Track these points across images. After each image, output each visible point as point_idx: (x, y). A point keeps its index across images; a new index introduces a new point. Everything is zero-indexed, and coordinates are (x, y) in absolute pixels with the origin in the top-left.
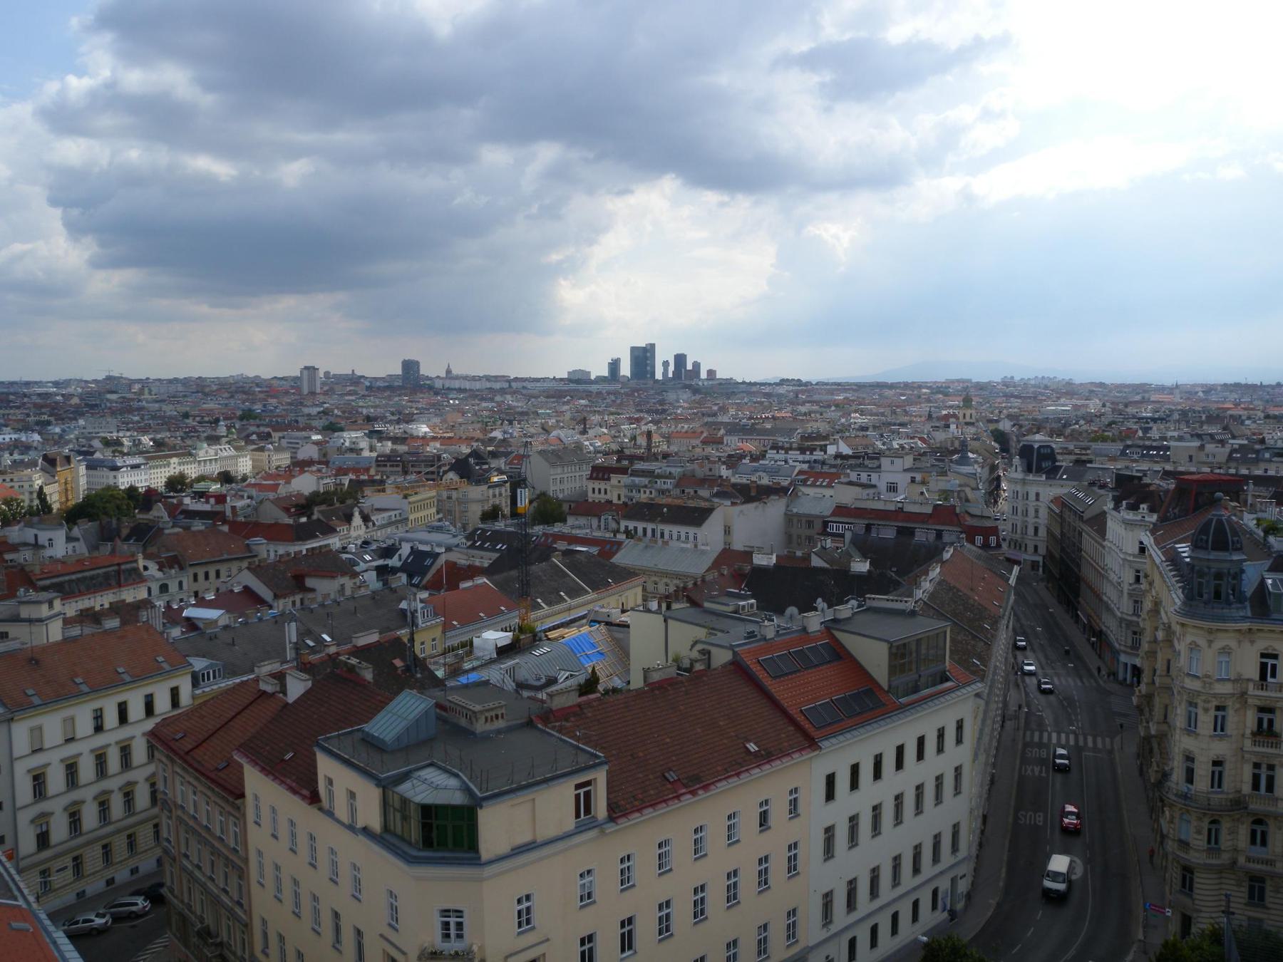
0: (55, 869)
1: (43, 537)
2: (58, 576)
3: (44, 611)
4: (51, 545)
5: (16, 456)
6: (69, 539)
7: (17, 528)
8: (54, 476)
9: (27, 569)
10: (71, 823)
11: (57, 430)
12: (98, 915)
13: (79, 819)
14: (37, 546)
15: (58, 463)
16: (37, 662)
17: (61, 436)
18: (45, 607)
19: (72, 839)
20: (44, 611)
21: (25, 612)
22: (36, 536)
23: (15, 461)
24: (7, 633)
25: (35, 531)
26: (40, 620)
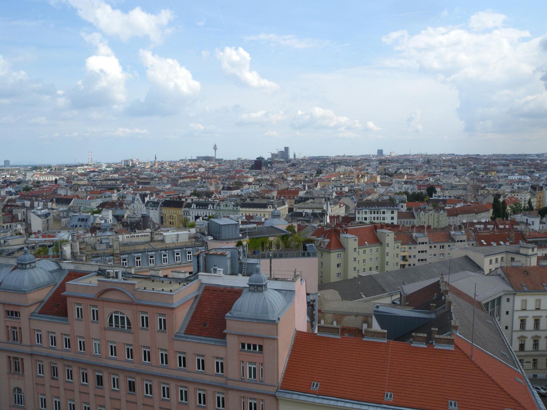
0: (525, 361)
1: (530, 220)
2: (536, 238)
3: (530, 252)
4: (533, 224)
5: (520, 185)
6: (541, 223)
7: (519, 215)
8: (535, 195)
9: (523, 233)
10: (534, 344)
11: (537, 175)
12: (542, 388)
13: (538, 344)
14: (527, 224)
15: (537, 189)
16: (527, 273)
17: (539, 178)
18: (530, 250)
19: (534, 351)
20: (530, 252)
21: (523, 251)
22: (527, 220)
23: (519, 188)
24: (514, 258)
25: (527, 218)
26: (526, 255)
